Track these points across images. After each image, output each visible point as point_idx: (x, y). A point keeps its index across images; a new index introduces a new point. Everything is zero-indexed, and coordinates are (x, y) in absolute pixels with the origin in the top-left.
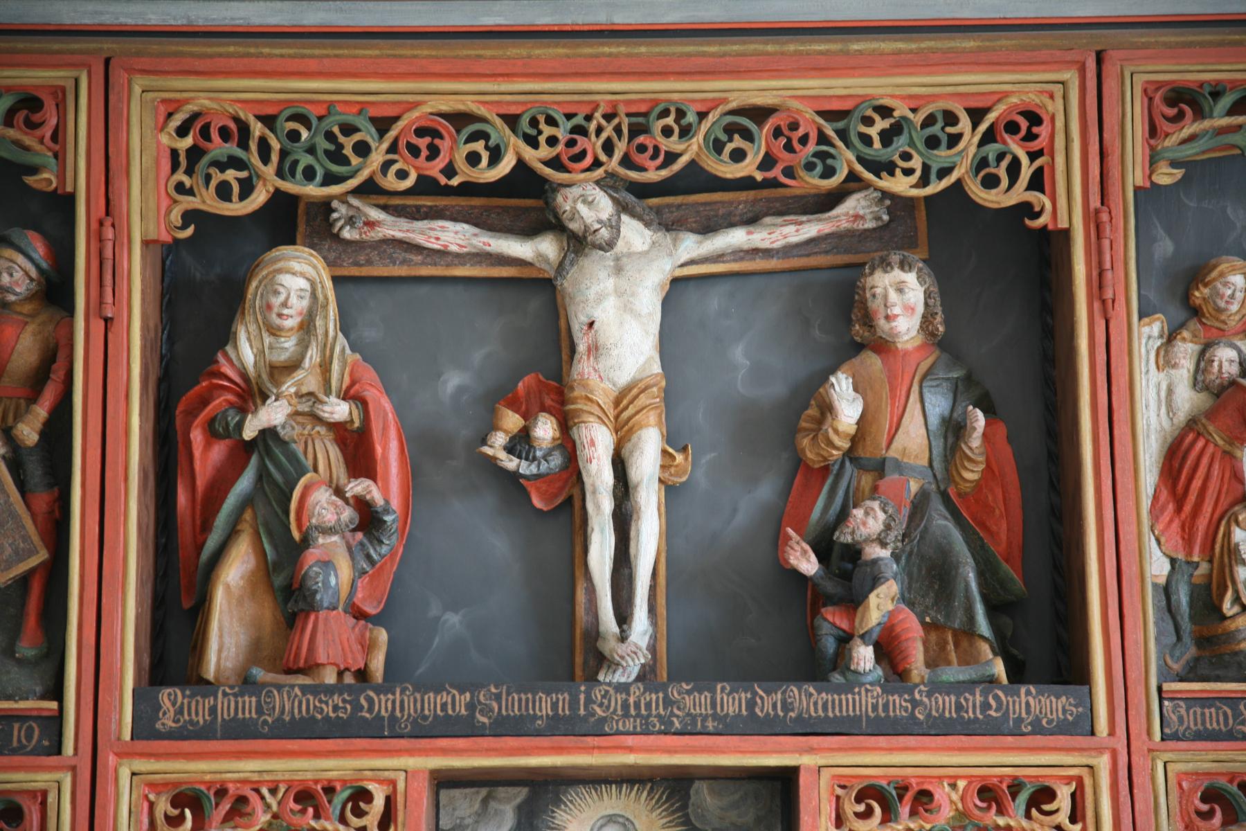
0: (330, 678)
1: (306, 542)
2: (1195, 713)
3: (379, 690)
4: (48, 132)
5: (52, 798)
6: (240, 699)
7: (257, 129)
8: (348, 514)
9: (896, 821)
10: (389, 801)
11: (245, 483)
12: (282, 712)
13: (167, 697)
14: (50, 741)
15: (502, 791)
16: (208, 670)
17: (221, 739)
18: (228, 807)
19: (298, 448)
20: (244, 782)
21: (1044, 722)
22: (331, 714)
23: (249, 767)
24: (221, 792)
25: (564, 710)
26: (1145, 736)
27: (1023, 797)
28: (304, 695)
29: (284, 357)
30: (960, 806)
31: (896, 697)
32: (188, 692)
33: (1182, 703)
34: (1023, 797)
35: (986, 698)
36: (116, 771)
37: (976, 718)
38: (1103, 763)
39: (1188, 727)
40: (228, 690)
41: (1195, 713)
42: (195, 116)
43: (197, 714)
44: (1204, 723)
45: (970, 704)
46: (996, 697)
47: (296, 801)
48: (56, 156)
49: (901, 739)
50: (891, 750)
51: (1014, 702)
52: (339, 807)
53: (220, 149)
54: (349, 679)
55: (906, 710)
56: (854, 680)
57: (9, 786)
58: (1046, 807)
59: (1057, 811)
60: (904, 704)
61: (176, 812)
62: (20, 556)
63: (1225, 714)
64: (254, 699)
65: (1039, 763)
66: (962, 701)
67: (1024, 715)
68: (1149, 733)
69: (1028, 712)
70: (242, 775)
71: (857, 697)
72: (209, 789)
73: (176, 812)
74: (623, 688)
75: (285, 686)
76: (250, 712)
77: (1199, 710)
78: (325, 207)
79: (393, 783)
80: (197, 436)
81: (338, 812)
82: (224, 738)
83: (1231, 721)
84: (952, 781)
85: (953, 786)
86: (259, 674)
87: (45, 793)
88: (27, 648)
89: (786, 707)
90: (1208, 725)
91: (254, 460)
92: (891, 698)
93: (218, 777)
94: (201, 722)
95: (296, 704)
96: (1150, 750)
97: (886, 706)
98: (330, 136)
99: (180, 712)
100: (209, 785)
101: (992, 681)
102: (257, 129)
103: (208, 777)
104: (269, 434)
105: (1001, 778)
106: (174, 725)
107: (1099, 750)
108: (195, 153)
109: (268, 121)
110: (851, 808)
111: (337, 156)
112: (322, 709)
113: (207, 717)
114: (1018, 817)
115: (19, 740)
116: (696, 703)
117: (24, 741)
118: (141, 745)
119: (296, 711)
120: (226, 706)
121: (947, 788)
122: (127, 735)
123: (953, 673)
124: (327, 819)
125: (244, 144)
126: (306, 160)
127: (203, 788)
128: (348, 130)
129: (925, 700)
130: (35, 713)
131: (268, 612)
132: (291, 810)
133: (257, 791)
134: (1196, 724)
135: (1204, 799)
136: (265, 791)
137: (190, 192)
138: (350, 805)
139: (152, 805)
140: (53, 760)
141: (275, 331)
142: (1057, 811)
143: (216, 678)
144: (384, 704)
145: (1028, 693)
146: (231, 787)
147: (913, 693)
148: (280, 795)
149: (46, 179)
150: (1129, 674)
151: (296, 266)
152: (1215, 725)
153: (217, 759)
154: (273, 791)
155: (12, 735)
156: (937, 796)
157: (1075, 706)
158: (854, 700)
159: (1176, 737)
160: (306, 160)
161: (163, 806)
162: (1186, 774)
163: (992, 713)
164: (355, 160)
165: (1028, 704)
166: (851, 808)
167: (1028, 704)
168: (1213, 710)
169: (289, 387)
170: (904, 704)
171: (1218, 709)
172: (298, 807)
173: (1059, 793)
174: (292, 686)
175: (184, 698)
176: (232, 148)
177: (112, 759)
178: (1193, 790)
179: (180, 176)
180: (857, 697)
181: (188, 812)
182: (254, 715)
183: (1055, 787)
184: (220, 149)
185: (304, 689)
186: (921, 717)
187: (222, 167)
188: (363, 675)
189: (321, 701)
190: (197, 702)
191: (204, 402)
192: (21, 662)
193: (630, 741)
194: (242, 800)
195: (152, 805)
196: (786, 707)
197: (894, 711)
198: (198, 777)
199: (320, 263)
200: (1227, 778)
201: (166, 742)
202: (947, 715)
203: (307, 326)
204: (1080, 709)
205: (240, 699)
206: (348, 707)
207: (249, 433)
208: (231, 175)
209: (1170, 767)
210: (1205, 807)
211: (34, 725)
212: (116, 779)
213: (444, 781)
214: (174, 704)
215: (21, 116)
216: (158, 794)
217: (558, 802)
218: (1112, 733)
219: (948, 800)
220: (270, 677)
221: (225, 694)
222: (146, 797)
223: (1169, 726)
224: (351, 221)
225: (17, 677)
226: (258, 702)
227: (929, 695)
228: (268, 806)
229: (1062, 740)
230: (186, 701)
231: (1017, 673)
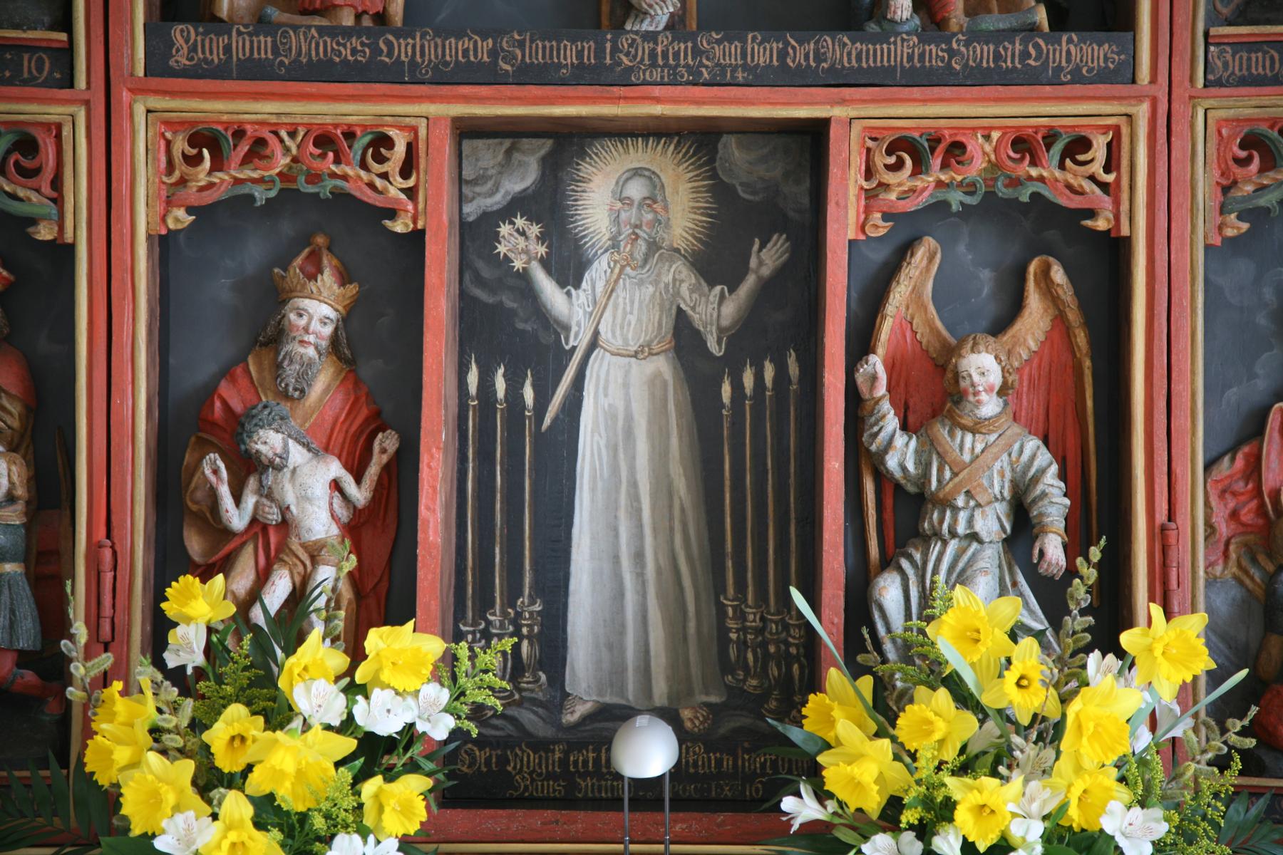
0: (348, 20)
2: (1241, 58)
3: (399, 34)
5: (66, 131)
6: (255, 39)
9: (927, 173)
10: (411, 148)
12: (299, 54)
13: (182, 34)
14: (62, 73)
15: (526, 143)
16: (221, 9)
17: (238, 79)
18: (247, 148)
20: (262, 123)
21: (1084, 71)
22: (350, 58)
23: (267, 109)
24: (239, 134)
25: (589, 58)
26: (1187, 84)
27: (1058, 148)
28: (321, 36)
30: (993, 157)
31: (933, 46)
32: (201, 30)
33: (1228, 49)
34: (1058, 148)
35: (1027, 47)
36: (131, 107)
37: (1015, 68)
38: (1142, 112)
39: (1233, 73)
40: (242, 29)
41: (1241, 58)
43: (211, 53)
44: (1249, 68)
45: (1009, 54)
46: (1037, 46)
47: (316, 145)
49: (936, 89)
50: (924, 101)
51: (1055, 50)
52: (360, 152)
54: (367, 22)
55: (942, 60)
56: (889, 29)
57: (22, 117)
58: (1081, 158)
59: (1092, 160)
60: (940, 54)
61: (194, 151)
63: (1272, 58)
64: (269, 39)
65: (1076, 112)
66: (1001, 49)
67: (1064, 64)
68: (1192, 80)
69: (1068, 61)
70: (259, 117)
71: (892, 47)
72: (226, 130)
73: (194, 151)
74: (651, 37)
75: (301, 27)
76: (266, 53)
77: (1245, 55)
79: (415, 130)
81: (358, 158)
82: (242, 77)
83: (1277, 65)
84: (986, 132)
85: (987, 137)
86: (274, 13)
87: (59, 127)
89: (819, 58)
90: (1254, 71)
92: (927, 48)
93: (235, 117)
94: (216, 61)
95: (313, 45)
96: (1191, 97)
97: (922, 56)
99: (193, 49)
100: (227, 125)
101: (1033, 29)
103: (225, 118)
105: (1037, 129)
106: (187, 63)
107: (1139, 99)
110: (881, 160)
112: (340, 52)
113: (222, 56)
114: (1052, 168)
115: (30, 72)
116: (727, 53)
117: (35, 72)
118: (155, 82)
119: (313, 53)
120: (241, 46)
121: (980, 140)
122: (140, 71)
123: (993, 21)
124: (348, 164)
127: (220, 128)
129: (963, 49)
130: (44, 44)
132: (311, 154)
133: (276, 134)
134: (1241, 70)
135: (1242, 146)
136: (283, 134)
138: (370, 151)
139: (169, 143)
140: (65, 93)
142: (1092, 160)
143: (230, 17)
144: (404, 49)
145: (1070, 41)
146: (249, 128)
147: (951, 43)
148: (300, 138)
150: (1175, 18)
152: (1260, 70)
153: (233, 99)
154: (292, 135)
155: (22, 65)
156: (969, 148)
157: (1118, 54)
158: (889, 50)
159: (1219, 83)
161: (181, 145)
162: (1226, 120)
163: (1032, 62)
165: (1068, 52)
166: (881, 160)
167: (1068, 52)
168: (1260, 54)
170: (940, 54)
171: (1265, 53)
172: (318, 151)
173: (1095, 143)
174: (309, 27)
175: (197, 35)
177: (125, 94)
178: (1232, 137)
180: (892, 47)
181: (206, 152)
182: (270, 56)
183: (1091, 137)
185: (320, 30)
186: (958, 67)
188: (381, 18)
189: (338, 44)
190: (211, 40)
193: (657, 91)
194: (260, 142)
195: (169, 143)
196: (819, 58)
197: (930, 61)
198: (214, 117)
200: (1268, 124)
201: (180, 80)
202: (985, 65)
204: (1122, 57)
205: (255, 39)
206: (367, 50)
209: (1210, 114)
210: (1243, 154)
211: (44, 56)
212: (131, 116)
213: (467, 130)
214: (187, 41)
216: (175, 133)
217: (583, 154)
218: (1153, 80)
219: (980, 152)
220: (285, 17)
221: (239, 33)
222: (163, 135)
223: (1213, 72)
226: (274, 43)
227: (967, 45)
228: (288, 150)
229: (1103, 89)
230: (199, 38)
231: (1060, 22)
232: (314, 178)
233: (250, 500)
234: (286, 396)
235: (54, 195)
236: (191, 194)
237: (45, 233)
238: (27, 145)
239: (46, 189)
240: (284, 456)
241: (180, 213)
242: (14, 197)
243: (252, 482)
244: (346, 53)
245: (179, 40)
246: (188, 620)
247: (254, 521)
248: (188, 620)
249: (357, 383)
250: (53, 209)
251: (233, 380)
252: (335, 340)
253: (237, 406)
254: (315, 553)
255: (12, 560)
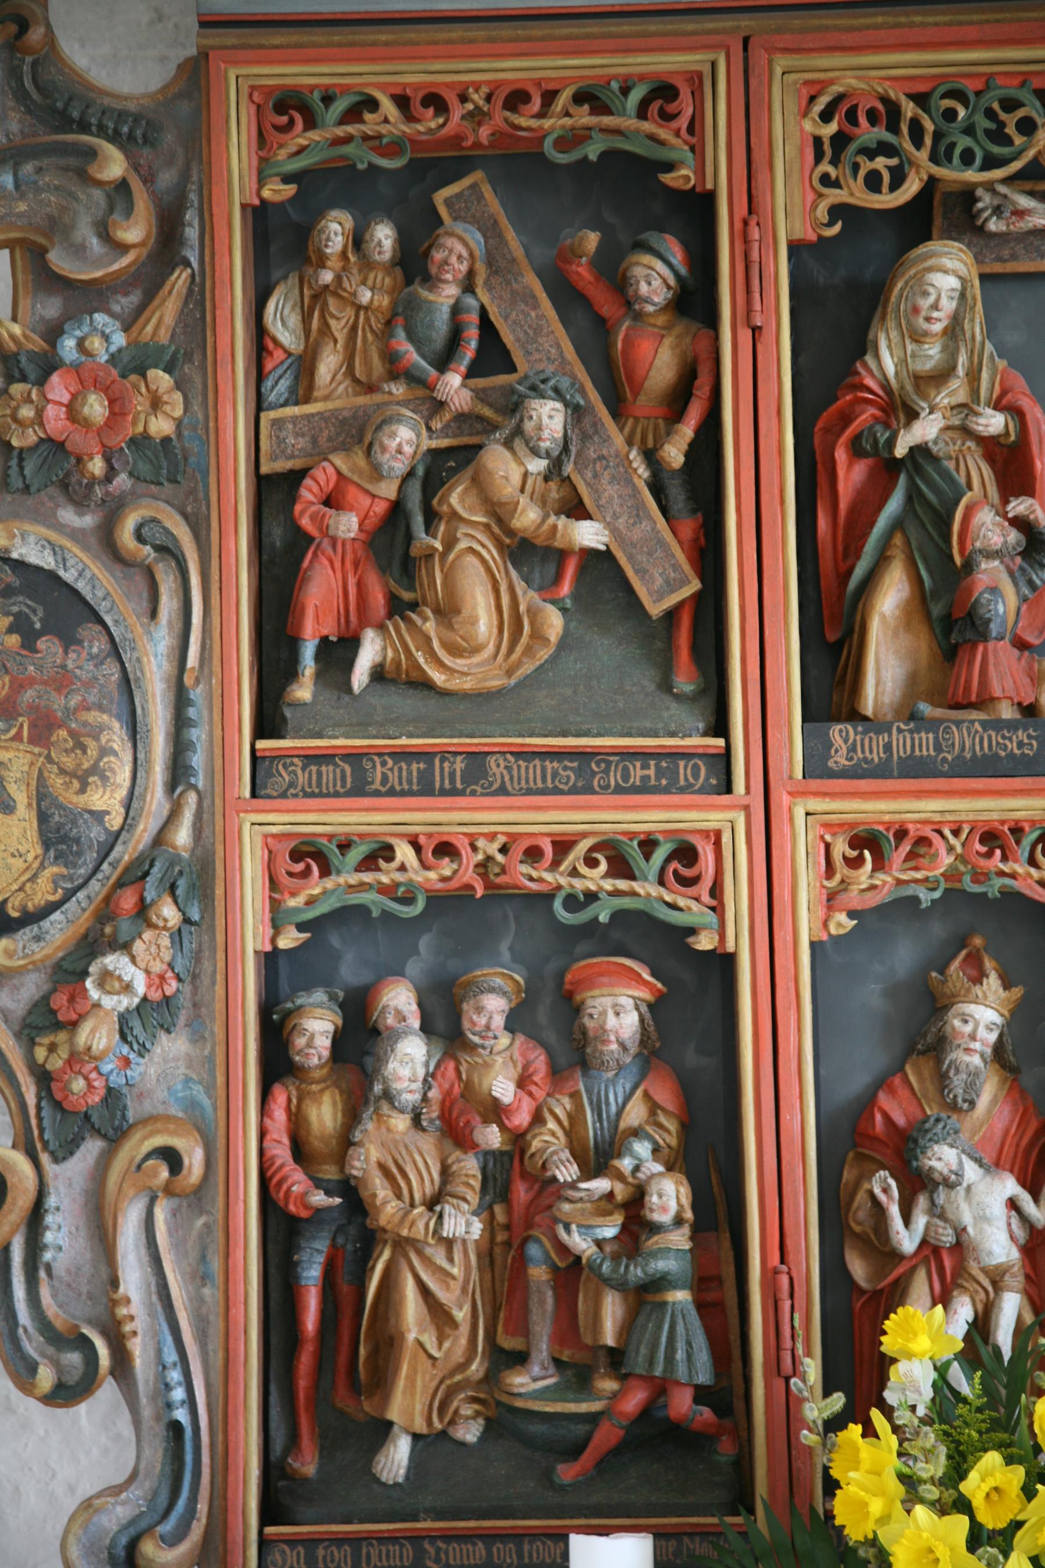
0: (1007, 712)
1: (969, 566)
4: (683, 122)
5: (726, 838)
6: (916, 736)
7: (909, 109)
8: (1014, 536)
11: (894, 504)
12: (963, 749)
13: (839, 733)
14: (718, 779)
16: (866, 706)
17: (898, 778)
18: (908, 848)
19: (951, 465)
20: (925, 822)
22: (1016, 751)
23: (930, 807)
24: (901, 834)
28: (985, 730)
29: (929, 365)
32: (860, 729)
36: (790, 810)
40: (902, 726)
42: (839, 98)
43: (871, 752)
47: (982, 841)
48: (693, 149)
52: (1028, 849)
53: (869, 134)
57: (681, 826)
61: (854, 853)
62: (672, 587)
64: (931, 736)
70: (923, 816)
72: (888, 830)
73: (854, 853)
75: (964, 721)
76: (928, 749)
78: (967, 196)
80: (841, 455)
81: (1026, 854)
82: (904, 775)
86: (925, 708)
87: (718, 834)
88: (685, 683)
91: (902, 480)
93: (897, 817)
94: (876, 760)
95: (977, 740)
98: (990, 114)
99: (853, 749)
100: (888, 825)
102: (909, 109)
103: (887, 818)
104: (920, 451)
106: (847, 763)
108: (840, 141)
109: (921, 99)
111: (999, 136)
112: (1006, 746)
113: (882, 755)
115: (686, 779)
117: (691, 780)
118: (815, 784)
119: (978, 748)
122: (799, 774)
124: (1016, 861)
125: (893, 127)
126: (963, 142)
127: (881, 828)
128: (1010, 105)
130: (701, 751)
131: (922, 644)
132: (977, 852)
133: (940, 832)
136: (947, 832)
137: (836, 184)
138: (1040, 847)
139: (828, 847)
140: (725, 799)
141: (918, 337)
143: (875, 714)
146: (911, 827)
148: (964, 836)
149: (682, 178)
151: (948, 263)
153: (895, 798)
154: (956, 833)
155: (678, 773)
160: (963, 142)
161: (841, 847)
164: (1018, 140)
169: (944, 398)
172: (983, 849)
174: (972, 722)
175: (856, 735)
176: (880, 133)
177: (785, 798)
179: (825, 167)
181: (867, 853)
182: (932, 753)
184: (869, 134)
185: (985, 725)
187: (871, 154)
189: (1004, 737)
190: (871, 739)
191: (846, 419)
192: (678, 698)
194: (923, 841)
195: (828, 847)
198: (875, 817)
199: (969, 258)
201: (841, 781)
203: (954, 330)
205: (916, 736)
206: (1034, 743)
207: (900, 451)
208: (881, 163)
211: (700, 763)
212: (791, 819)
214: (846, 741)
215: (654, 107)
216: (834, 834)
220: (939, 712)
221: (900, 731)
222: (822, 838)
224: (998, 211)
225: (676, 712)
226: (936, 739)
228: (951, 849)
230: (858, 738)
232: (979, 877)
233: (921, 1221)
234: (954, 1107)
235: (714, 903)
236: (854, 898)
237: (705, 942)
238: (686, 853)
239: (706, 898)
240: (959, 1174)
241: (842, 917)
242: (673, 907)
243: (922, 1201)
244: (1013, 746)
245: (837, 740)
246: (910, 1356)
247: (924, 1243)
248: (910, 1356)
249: (1022, 1092)
250: (712, 918)
251: (892, 1091)
252: (999, 1049)
253: (900, 1120)
254: (997, 1278)
255: (683, 1287)
